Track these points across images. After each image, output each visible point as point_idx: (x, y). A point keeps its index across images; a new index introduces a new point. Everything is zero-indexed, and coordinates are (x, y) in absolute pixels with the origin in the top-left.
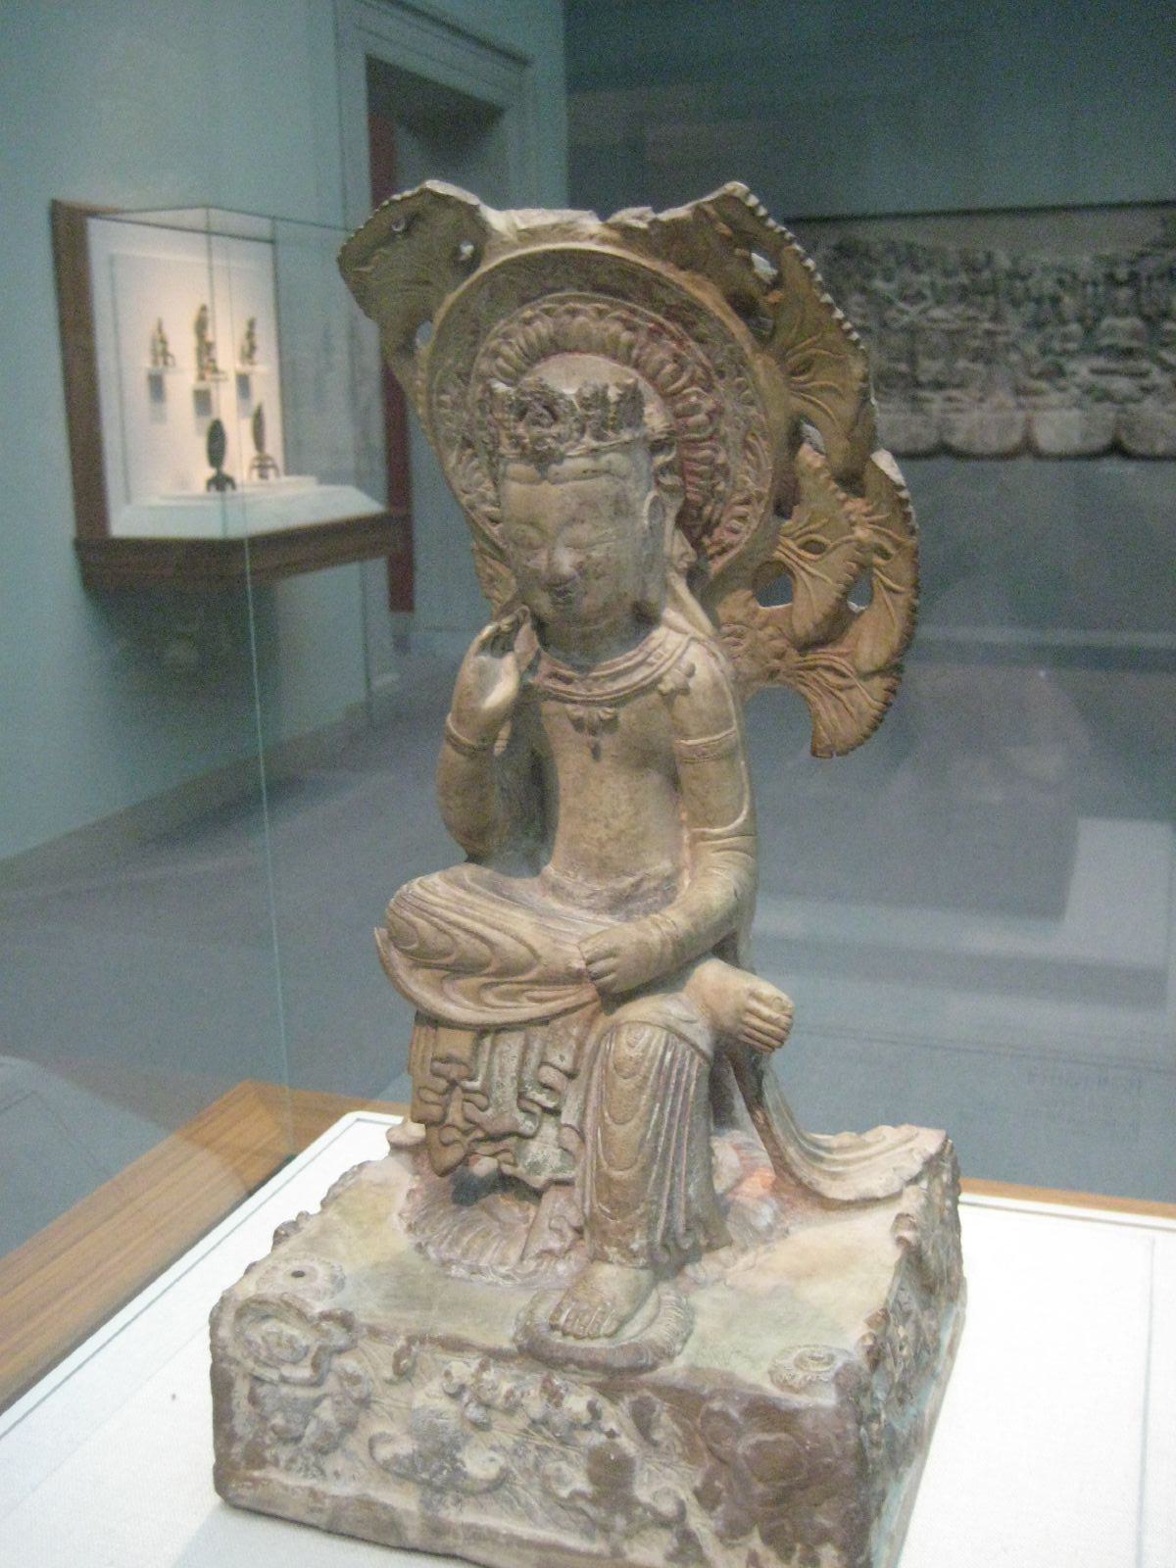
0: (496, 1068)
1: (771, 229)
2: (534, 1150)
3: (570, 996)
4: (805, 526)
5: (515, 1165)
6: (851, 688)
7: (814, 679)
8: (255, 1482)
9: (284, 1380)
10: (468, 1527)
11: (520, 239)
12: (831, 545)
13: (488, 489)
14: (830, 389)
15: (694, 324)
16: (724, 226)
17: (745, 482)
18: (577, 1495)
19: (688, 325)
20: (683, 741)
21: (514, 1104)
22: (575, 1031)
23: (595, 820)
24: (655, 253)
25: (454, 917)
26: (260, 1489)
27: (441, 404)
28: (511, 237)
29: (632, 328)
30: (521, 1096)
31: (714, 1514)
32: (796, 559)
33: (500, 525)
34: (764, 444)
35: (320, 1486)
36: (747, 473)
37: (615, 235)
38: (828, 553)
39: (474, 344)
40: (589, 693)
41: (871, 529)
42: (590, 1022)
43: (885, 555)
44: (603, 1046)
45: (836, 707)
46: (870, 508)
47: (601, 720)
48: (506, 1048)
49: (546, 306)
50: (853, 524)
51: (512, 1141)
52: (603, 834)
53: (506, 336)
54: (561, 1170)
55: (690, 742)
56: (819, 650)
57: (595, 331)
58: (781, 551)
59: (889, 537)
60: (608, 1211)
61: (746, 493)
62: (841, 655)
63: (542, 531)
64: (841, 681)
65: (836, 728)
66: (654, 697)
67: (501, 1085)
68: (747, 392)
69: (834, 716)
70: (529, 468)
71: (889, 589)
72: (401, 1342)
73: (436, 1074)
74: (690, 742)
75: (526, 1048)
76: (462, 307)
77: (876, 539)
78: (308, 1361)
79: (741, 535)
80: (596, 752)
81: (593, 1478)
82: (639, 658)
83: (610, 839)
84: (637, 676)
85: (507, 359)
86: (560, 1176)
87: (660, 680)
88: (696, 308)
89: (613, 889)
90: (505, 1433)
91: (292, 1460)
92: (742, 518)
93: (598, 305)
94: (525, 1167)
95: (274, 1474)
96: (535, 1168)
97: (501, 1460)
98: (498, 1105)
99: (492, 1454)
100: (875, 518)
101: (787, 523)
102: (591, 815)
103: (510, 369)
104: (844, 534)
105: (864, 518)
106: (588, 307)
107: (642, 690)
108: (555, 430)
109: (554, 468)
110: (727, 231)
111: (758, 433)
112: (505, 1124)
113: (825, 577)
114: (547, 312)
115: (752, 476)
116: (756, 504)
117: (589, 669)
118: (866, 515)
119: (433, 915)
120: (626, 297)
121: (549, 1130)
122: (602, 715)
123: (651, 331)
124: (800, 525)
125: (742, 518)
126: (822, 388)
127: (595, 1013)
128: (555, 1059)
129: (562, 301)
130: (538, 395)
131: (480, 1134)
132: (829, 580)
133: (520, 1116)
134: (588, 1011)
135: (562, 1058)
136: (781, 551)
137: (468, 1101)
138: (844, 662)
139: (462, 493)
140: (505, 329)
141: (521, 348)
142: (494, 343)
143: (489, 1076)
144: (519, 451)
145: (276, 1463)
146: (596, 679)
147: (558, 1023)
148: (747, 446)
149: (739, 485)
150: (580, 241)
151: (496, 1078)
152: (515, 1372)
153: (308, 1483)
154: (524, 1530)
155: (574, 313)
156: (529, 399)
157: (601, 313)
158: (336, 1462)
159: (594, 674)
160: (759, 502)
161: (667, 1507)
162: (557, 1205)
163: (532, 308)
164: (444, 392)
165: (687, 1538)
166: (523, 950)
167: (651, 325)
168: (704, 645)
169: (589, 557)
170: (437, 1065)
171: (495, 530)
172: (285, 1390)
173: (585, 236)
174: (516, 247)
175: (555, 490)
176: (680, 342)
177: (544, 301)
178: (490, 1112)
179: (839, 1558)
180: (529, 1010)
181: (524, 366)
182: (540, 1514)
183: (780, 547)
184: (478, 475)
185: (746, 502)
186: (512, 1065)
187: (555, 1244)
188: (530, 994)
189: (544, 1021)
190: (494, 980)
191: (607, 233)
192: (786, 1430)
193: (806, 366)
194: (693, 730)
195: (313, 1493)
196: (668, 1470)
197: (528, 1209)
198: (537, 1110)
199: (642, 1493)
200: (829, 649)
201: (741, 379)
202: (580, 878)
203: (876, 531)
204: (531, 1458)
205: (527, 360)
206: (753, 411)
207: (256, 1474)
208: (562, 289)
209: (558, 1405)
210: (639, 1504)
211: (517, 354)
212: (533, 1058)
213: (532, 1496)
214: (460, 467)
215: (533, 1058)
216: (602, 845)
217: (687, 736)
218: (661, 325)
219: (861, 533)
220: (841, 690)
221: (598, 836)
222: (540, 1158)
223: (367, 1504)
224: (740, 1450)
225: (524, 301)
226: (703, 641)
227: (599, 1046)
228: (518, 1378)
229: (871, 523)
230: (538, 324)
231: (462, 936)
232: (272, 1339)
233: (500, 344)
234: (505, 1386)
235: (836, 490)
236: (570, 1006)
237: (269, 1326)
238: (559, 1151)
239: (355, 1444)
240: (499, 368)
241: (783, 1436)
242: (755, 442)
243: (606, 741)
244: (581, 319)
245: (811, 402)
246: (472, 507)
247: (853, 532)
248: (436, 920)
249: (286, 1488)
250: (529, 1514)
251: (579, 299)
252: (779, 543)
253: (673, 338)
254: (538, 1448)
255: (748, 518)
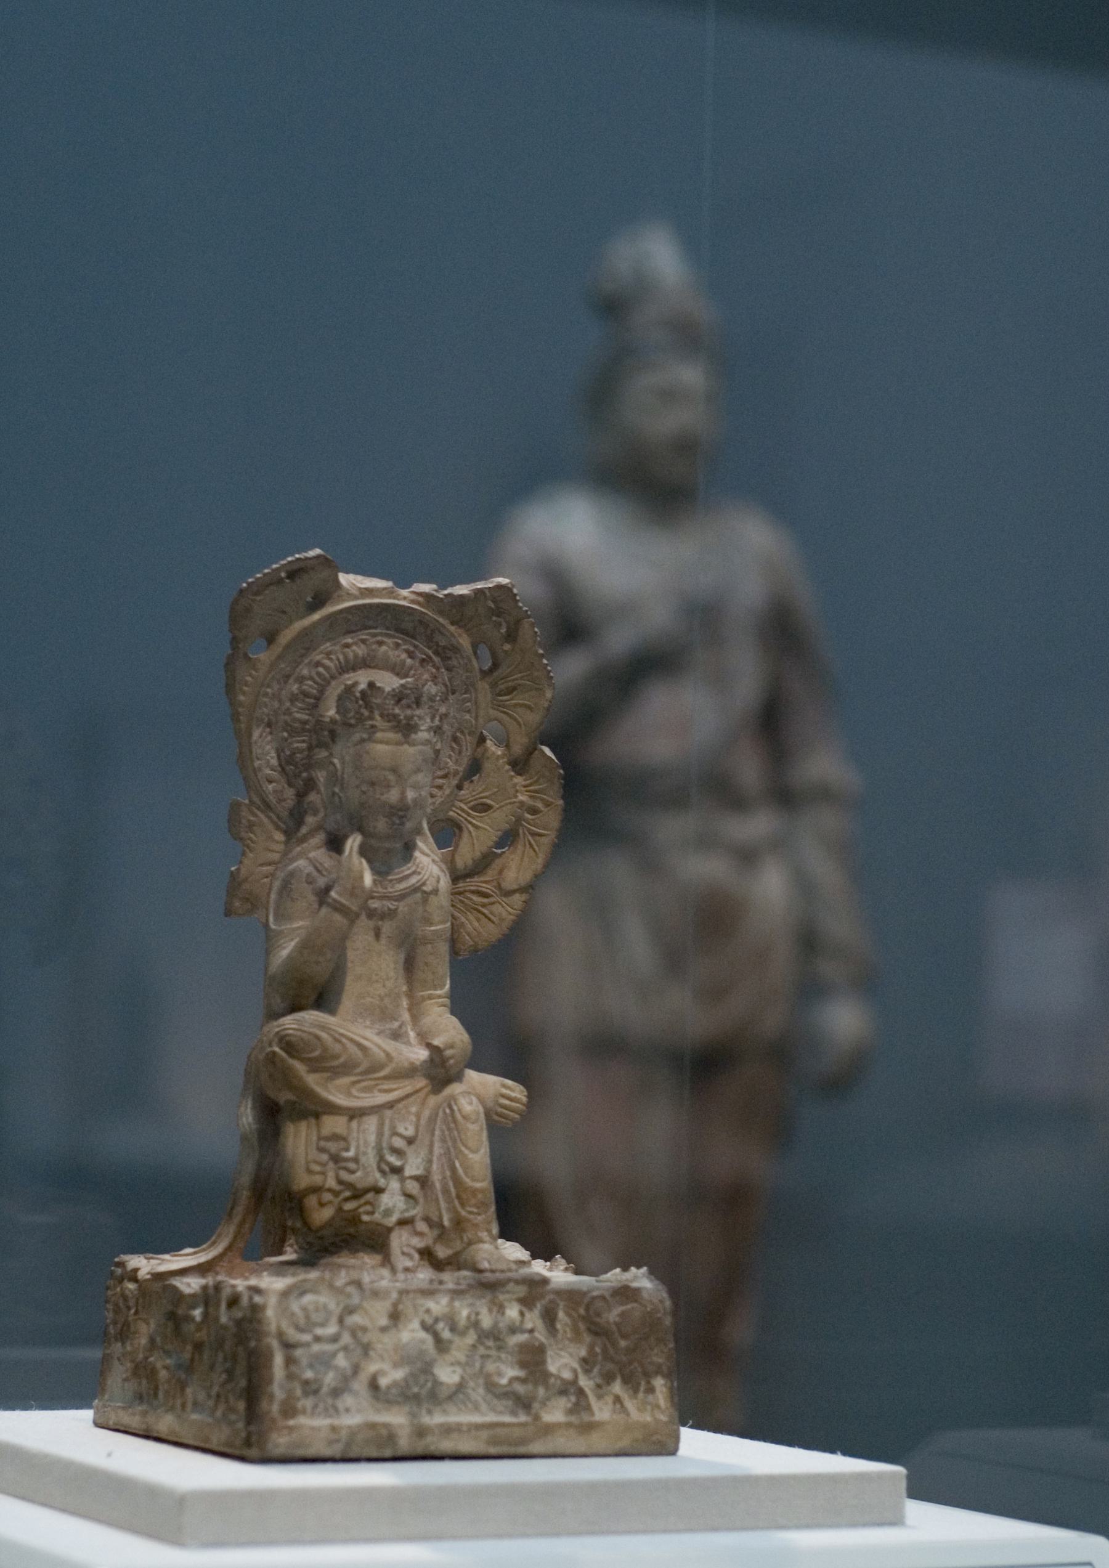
0: (361, 1142)
1: (521, 608)
2: (386, 1200)
3: (407, 1087)
4: (481, 793)
5: (372, 1213)
6: (493, 903)
7: (461, 901)
8: (291, 1429)
9: (318, 1339)
10: (442, 1425)
11: (361, 593)
12: (497, 806)
13: (272, 758)
14: (521, 705)
15: (450, 658)
16: (491, 603)
17: (447, 763)
18: (512, 1380)
19: (445, 659)
20: (428, 928)
21: (375, 1166)
22: (414, 1109)
23: (377, 981)
24: (441, 613)
25: (342, 1031)
26: (294, 1436)
27: (266, 695)
28: (355, 592)
29: (411, 655)
30: (381, 1159)
31: (592, 1375)
32: (466, 816)
33: (274, 784)
34: (468, 738)
35: (336, 1422)
36: (450, 757)
37: (420, 599)
38: (495, 811)
39: (302, 656)
40: (385, 891)
41: (528, 795)
42: (423, 1103)
43: (534, 811)
44: (441, 1113)
45: (478, 920)
46: (528, 782)
47: (389, 909)
48: (367, 1126)
49: (364, 637)
50: (517, 791)
51: (370, 1196)
52: (382, 991)
53: (328, 654)
54: (407, 1210)
55: (432, 928)
56: (468, 880)
57: (392, 656)
58: (454, 811)
59: (542, 800)
60: (475, 1210)
61: (447, 770)
62: (485, 882)
63: (399, 776)
64: (486, 900)
65: (479, 933)
66: (419, 895)
67: (365, 1153)
68: (468, 704)
69: (476, 924)
70: (396, 735)
71: (534, 834)
72: (394, 1295)
73: (322, 1150)
74: (432, 928)
75: (381, 1125)
76: (305, 632)
77: (531, 802)
78: (334, 1320)
79: (436, 798)
80: (377, 934)
81: (523, 1365)
82: (413, 869)
83: (386, 995)
84: (413, 880)
85: (326, 668)
86: (407, 1215)
87: (424, 884)
88: (456, 649)
89: (390, 1029)
90: (461, 1347)
91: (315, 1406)
92: (440, 787)
93: (397, 640)
94: (379, 1213)
95: (302, 1420)
96: (388, 1213)
97: (459, 1370)
98: (365, 1168)
99: (452, 1368)
100: (532, 788)
101: (462, 792)
102: (374, 978)
103: (327, 675)
104: (510, 798)
105: (523, 789)
106: (390, 641)
107: (416, 889)
108: (418, 712)
109: (413, 736)
110: (493, 606)
111: (466, 731)
112: (369, 1182)
113: (488, 827)
114: (363, 641)
115: (453, 759)
116: (451, 778)
117: (388, 873)
118: (525, 786)
119: (330, 1029)
120: (413, 637)
121: (394, 1184)
122: (391, 906)
123: (423, 660)
124: (474, 793)
125: (440, 787)
126: (515, 705)
127: (427, 1095)
128: (401, 1130)
129: (375, 635)
130: (414, 690)
131: (347, 1194)
132: (491, 830)
133: (378, 1175)
134: (422, 1094)
135: (406, 1129)
136: (454, 811)
137: (340, 1168)
138: (489, 887)
139: (256, 760)
140: (330, 649)
141: (340, 662)
142: (318, 658)
143: (358, 1147)
144: (394, 723)
145: (304, 1412)
146: (391, 881)
147: (400, 1105)
148: (455, 739)
149: (442, 765)
150: (398, 600)
151: (362, 1149)
152: (470, 1301)
153: (327, 1422)
154: (477, 1419)
155: (381, 643)
156: (409, 692)
157: (397, 645)
158: (348, 1400)
159: (390, 878)
160: (454, 776)
161: (567, 1375)
162: (404, 1239)
163: (352, 638)
164: (269, 686)
165: (581, 1392)
166: (382, 1055)
167: (424, 657)
168: (437, 865)
169: (420, 795)
170: (322, 1143)
171: (270, 787)
172: (316, 1348)
173: (401, 597)
174: (356, 598)
175: (412, 750)
176: (438, 669)
177: (362, 634)
178: (359, 1174)
179: (665, 1385)
180: (381, 1099)
181: (337, 674)
182: (484, 1407)
183: (454, 809)
184: (268, 747)
185: (445, 776)
186: (372, 1138)
187: (409, 1264)
188: (380, 1087)
189: (390, 1105)
190: (360, 1078)
191: (413, 597)
192: (636, 1301)
193: (510, 691)
194: (436, 919)
195: (334, 1429)
196: (563, 1353)
197: (363, 1257)
198: (387, 1169)
199: (552, 1368)
200: (476, 879)
201: (465, 696)
202: (368, 1023)
203: (531, 797)
204: (478, 1365)
205: (340, 670)
206: (467, 717)
207: (291, 1422)
208: (376, 628)
209: (503, 1314)
210: (552, 1375)
211: (336, 666)
212: (387, 1132)
213: (478, 1393)
214: (260, 740)
215: (387, 1132)
216: (382, 999)
217: (431, 924)
218: (430, 658)
219: (521, 797)
220: (484, 905)
221: (378, 992)
222: (390, 1205)
223: (373, 1426)
224: (611, 1319)
225: (349, 632)
226: (437, 862)
227: (437, 1115)
228: (472, 1305)
229: (527, 791)
230: (354, 648)
231: (349, 1045)
232: (311, 1307)
233: (323, 658)
234: (465, 1313)
235: (507, 771)
236: (409, 1092)
237: (308, 1298)
238: (403, 1198)
239: (360, 1385)
240: (318, 674)
241: (635, 1305)
242: (462, 737)
243: (387, 927)
244: (384, 648)
245: (505, 713)
246: (260, 769)
247: (516, 797)
248: (332, 1033)
249: (313, 1429)
250: (476, 1408)
251: (381, 634)
252: (453, 805)
253: (434, 666)
254: (482, 1357)
255: (445, 787)
